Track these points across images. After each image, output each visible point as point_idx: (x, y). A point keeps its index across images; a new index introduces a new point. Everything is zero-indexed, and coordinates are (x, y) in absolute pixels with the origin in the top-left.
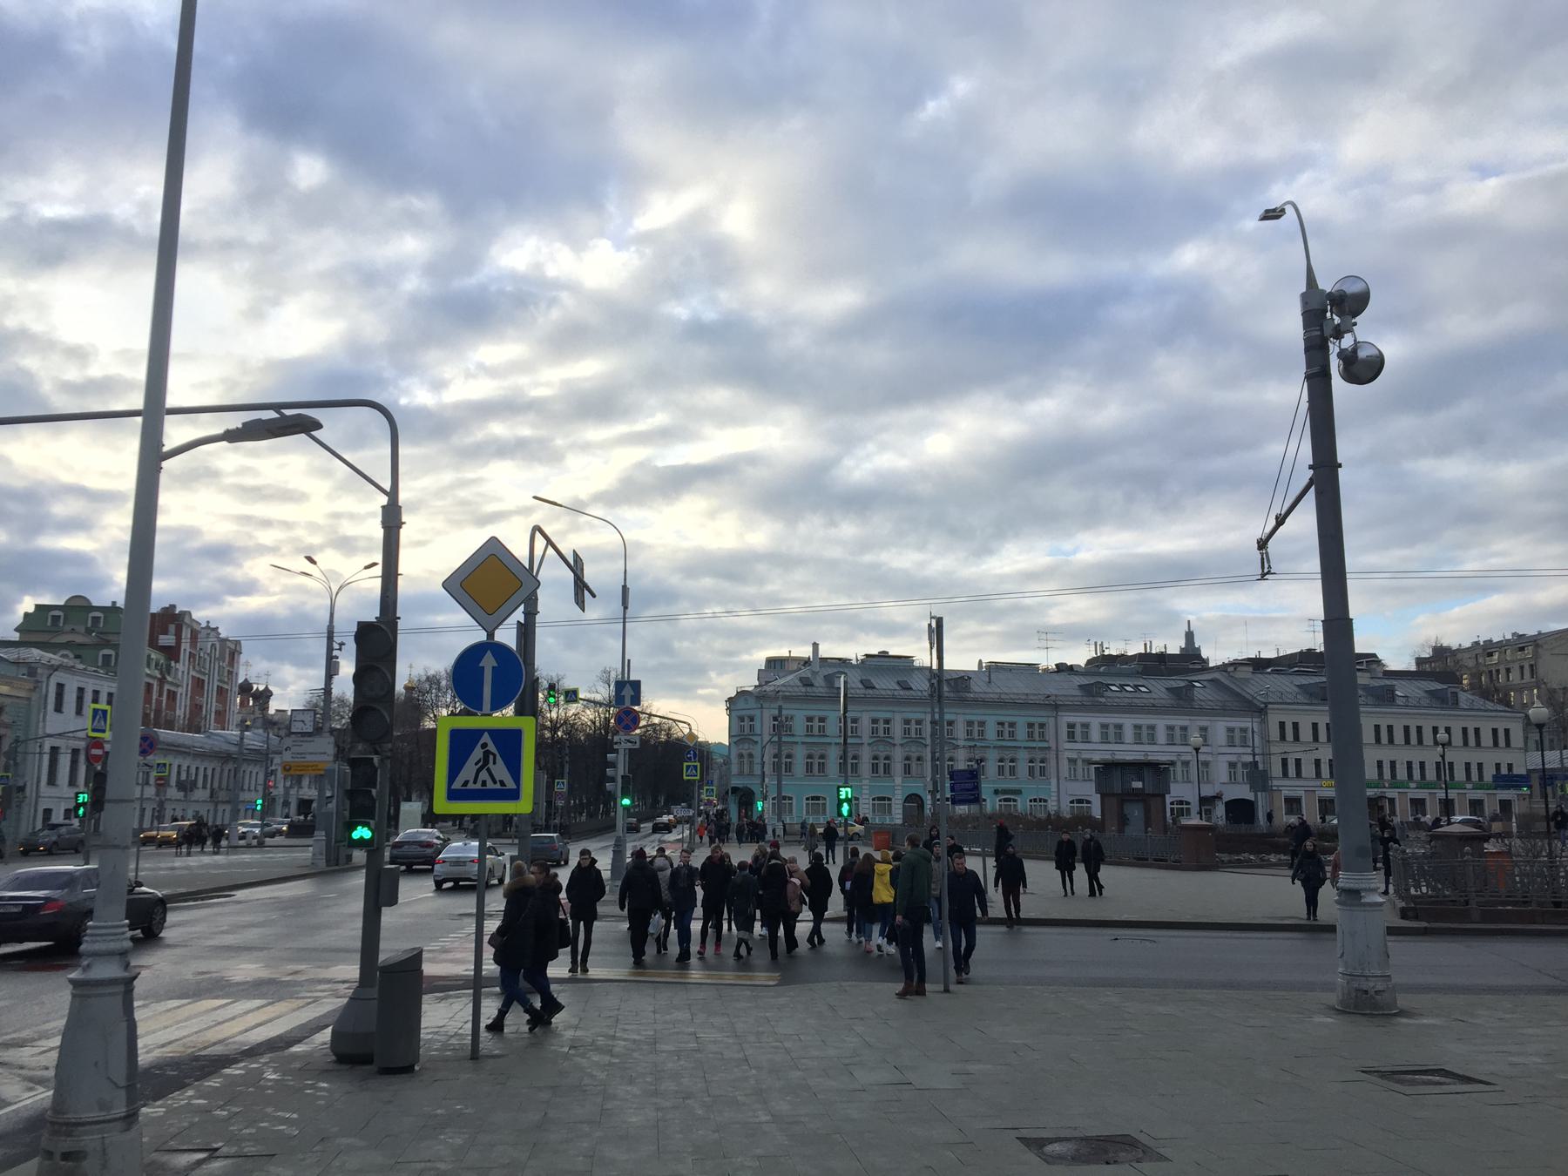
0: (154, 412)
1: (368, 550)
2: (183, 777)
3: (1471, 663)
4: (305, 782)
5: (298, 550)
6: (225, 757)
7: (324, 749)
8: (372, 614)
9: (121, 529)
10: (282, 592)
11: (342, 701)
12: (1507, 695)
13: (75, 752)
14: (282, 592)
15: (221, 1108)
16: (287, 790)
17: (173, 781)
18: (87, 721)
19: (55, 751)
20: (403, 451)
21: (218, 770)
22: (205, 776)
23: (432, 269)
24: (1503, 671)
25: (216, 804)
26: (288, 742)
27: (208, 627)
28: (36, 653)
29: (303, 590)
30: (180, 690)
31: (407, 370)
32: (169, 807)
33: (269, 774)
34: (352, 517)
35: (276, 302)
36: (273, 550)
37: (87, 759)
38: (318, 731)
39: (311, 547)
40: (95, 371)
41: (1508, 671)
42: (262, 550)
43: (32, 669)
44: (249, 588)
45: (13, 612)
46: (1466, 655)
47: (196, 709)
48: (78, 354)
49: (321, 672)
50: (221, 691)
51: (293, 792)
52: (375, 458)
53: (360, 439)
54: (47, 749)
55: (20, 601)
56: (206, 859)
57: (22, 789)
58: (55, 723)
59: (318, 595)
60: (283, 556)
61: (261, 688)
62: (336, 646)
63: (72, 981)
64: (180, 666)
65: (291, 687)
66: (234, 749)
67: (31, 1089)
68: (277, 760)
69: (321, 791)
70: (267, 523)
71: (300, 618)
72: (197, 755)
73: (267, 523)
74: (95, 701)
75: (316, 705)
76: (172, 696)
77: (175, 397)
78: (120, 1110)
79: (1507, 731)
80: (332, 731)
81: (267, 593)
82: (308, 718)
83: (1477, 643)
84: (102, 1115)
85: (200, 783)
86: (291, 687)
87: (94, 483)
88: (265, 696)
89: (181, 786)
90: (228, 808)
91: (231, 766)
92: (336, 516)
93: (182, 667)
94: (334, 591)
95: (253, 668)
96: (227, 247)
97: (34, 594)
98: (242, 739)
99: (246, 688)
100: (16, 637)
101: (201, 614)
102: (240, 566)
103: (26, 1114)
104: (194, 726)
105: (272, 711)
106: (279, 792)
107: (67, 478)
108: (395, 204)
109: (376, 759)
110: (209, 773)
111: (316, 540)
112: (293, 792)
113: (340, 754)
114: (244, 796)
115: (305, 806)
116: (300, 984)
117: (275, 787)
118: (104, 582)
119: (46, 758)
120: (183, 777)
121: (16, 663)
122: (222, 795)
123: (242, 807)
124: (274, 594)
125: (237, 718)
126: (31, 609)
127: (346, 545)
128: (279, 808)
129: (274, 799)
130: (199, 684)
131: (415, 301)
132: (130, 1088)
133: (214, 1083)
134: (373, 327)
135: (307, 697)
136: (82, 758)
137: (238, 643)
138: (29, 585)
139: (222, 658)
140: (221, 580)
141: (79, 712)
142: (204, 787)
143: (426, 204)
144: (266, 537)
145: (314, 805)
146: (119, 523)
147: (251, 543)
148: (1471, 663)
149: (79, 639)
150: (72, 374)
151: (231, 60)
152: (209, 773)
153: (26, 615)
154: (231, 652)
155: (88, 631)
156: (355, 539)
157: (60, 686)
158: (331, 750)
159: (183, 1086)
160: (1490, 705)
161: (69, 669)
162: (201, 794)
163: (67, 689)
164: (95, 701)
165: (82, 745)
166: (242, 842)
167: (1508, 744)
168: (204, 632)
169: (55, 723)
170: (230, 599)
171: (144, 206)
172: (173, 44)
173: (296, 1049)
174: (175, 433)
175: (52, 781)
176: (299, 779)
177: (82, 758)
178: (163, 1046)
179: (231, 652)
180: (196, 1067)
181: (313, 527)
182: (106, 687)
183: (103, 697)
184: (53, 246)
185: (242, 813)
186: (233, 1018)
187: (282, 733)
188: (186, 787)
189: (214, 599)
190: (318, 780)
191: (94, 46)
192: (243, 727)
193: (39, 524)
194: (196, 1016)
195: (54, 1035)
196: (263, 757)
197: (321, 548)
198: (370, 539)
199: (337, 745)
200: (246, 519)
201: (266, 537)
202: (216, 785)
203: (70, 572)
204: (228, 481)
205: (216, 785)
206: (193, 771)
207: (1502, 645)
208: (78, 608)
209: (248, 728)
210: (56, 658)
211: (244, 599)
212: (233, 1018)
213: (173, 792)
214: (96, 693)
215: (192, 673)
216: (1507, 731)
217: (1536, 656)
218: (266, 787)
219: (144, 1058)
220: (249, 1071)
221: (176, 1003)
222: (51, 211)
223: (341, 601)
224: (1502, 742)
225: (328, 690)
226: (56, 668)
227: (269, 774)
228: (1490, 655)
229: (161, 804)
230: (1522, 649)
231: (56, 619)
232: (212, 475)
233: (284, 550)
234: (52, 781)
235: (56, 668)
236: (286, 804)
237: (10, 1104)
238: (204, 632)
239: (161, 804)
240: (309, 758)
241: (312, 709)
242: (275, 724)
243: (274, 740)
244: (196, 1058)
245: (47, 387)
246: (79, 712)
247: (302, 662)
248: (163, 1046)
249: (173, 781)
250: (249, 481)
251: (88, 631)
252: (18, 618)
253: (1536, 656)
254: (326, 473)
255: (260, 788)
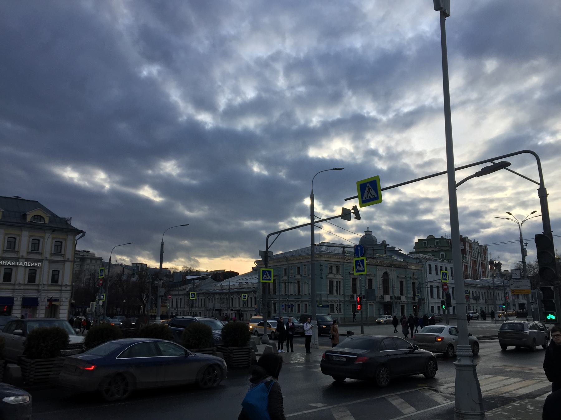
0: (451, 170)
1: (533, 205)
2: (475, 295)
4: (520, 297)
5: (505, 209)
6: (489, 288)
7: (526, 284)
8: (541, 231)
9: (444, 210)
10: (501, 225)
11: (530, 266)
13: (438, 287)
14: (501, 225)
15: (514, 417)
16: (514, 300)
17: (471, 297)
18: (441, 277)
19: (431, 287)
20: (542, 163)
21: (486, 292)
22: (482, 295)
23: (546, 87)
25: (488, 305)
26: (511, 282)
27: (474, 242)
28: (421, 255)
29: (511, 224)
30: (468, 265)
31: (541, 130)
32: (471, 306)
33: (506, 294)
34: (524, 193)
35: (484, 118)
36: (495, 210)
37: (443, 289)
38: (523, 277)
39: (510, 208)
40: (426, 159)
42: (491, 211)
43: (420, 260)
44: (489, 225)
45: (413, 242)
47: (475, 271)
48: (420, 154)
49: (520, 255)
50: (482, 264)
51: (516, 300)
52: (531, 169)
53: (522, 164)
54: (429, 286)
55: (414, 238)
56: (488, 325)
57: (424, 300)
58: (430, 278)
59: (515, 225)
60: (499, 212)
61: (497, 262)
62: (524, 245)
63: (457, 366)
64: (467, 256)
65: (509, 261)
66: (491, 285)
67: (445, 400)
68: (508, 289)
69: (528, 301)
70: (492, 201)
71: (508, 234)
72: (478, 287)
73: (492, 201)
74: (441, 270)
75: (520, 268)
76: (466, 267)
77: (458, 162)
78: (479, 412)
80: (528, 277)
81: (495, 226)
82: (518, 272)
84: (473, 413)
85: (481, 298)
86: (509, 261)
87: (430, 196)
88: (499, 265)
89: (474, 298)
90: (493, 306)
91: (490, 291)
92: (518, 193)
93: (468, 256)
94: (520, 222)
95: (493, 255)
96: (463, 103)
97: (419, 236)
98: (493, 281)
99: (491, 263)
100: (414, 250)
101: (471, 237)
102: (484, 218)
103: (446, 409)
104: (475, 277)
105: (502, 271)
106: (510, 300)
107: (422, 196)
108: (526, 66)
109: (552, 288)
110: (484, 294)
111: (510, 204)
112: (516, 300)
113: (533, 287)
114: (498, 302)
115: (522, 306)
116: (532, 374)
117: (509, 299)
118: (439, 229)
119: (429, 289)
120: (475, 295)
121: (416, 259)
122: (489, 302)
123: (498, 306)
124: (498, 227)
125: (490, 274)
126: (417, 241)
127: (524, 205)
128: (512, 307)
129: (509, 303)
130: (474, 262)
131: (540, 102)
132: (481, 404)
133: (509, 407)
134: (523, 116)
135: (516, 264)
136: (441, 289)
137: (486, 246)
138: (417, 233)
139: (481, 252)
140: (478, 224)
141: (437, 274)
142: (483, 299)
143: (540, 61)
144: (492, 206)
145: (525, 306)
146: (444, 208)
147: (487, 209)
149: (434, 250)
150: (420, 161)
151: (457, 36)
152: (484, 294)
153: (416, 243)
154: (484, 250)
155: (435, 247)
156: (528, 201)
157: (430, 265)
158: (529, 284)
159: (497, 407)
161: (432, 260)
162: (482, 301)
163: (432, 266)
164: (441, 270)
165: (440, 285)
166: (500, 319)
168: (473, 244)
169: (430, 278)
170: (482, 230)
171: (435, 99)
172: (439, 39)
173: (537, 399)
174: (459, 176)
175: (432, 297)
176: (518, 295)
177: (441, 289)
178: (487, 391)
179: (484, 250)
180: (501, 401)
181: (509, 199)
182: (449, 266)
183: (444, 268)
184: (407, 122)
185: (498, 309)
186: (511, 384)
187: (508, 278)
188: (476, 299)
189: (476, 231)
190: (526, 296)
191: (412, 52)
192: (493, 277)
193: (416, 212)
194: (496, 382)
195: (451, 382)
196: (502, 288)
197: (514, 207)
198: (533, 200)
199: (531, 283)
200: (484, 200)
201: (492, 206)
202: (487, 298)
203: (428, 227)
204: (476, 187)
205: (487, 298)
206: (478, 293)
208: (431, 239)
209: (495, 277)
210: (427, 256)
211: (487, 230)
212: (511, 384)
213: (472, 301)
214: (441, 267)
215: (472, 258)
218: (506, 299)
219: (483, 394)
220: (521, 405)
221: (488, 376)
222: (406, 110)
223: (524, 226)
225: (524, 261)
226: (428, 260)
227: (506, 294)
229: (469, 305)
231: (425, 243)
232: (470, 186)
233: (500, 209)
234: (432, 297)
235: (428, 260)
236: (514, 305)
237: (440, 404)
238: (473, 244)
239: (469, 305)
240: (521, 288)
241: (518, 269)
242: (505, 275)
243: (505, 281)
244: (500, 397)
245: (413, 168)
246: (437, 274)
247: (512, 251)
248: (487, 391)
249: (471, 297)
250: (483, 186)
251: (435, 247)
252: (414, 244)
254: (511, 178)
255: (503, 299)
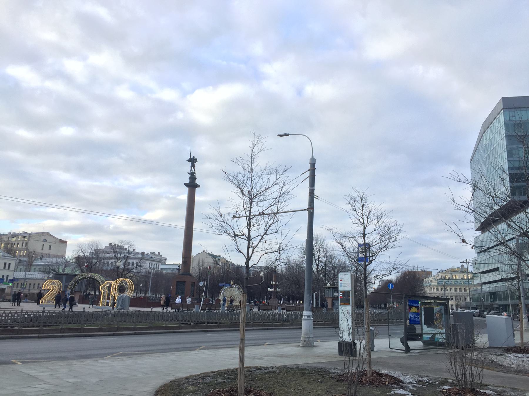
3: (6, 240)
12: (15, 252)
24: (16, 244)
41: (18, 244)
46: (5, 237)
79: (10, 264)
83: (10, 233)
148: (6, 240)
160: (9, 255)
167: (9, 268)
207: (20, 234)
216: (10, 264)
217: (29, 240)
224: (7, 268)
228: (14, 237)
230: (25, 237)
253: (29, 240)
